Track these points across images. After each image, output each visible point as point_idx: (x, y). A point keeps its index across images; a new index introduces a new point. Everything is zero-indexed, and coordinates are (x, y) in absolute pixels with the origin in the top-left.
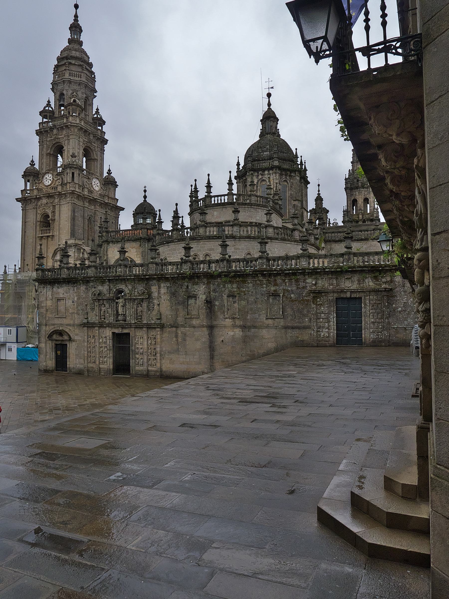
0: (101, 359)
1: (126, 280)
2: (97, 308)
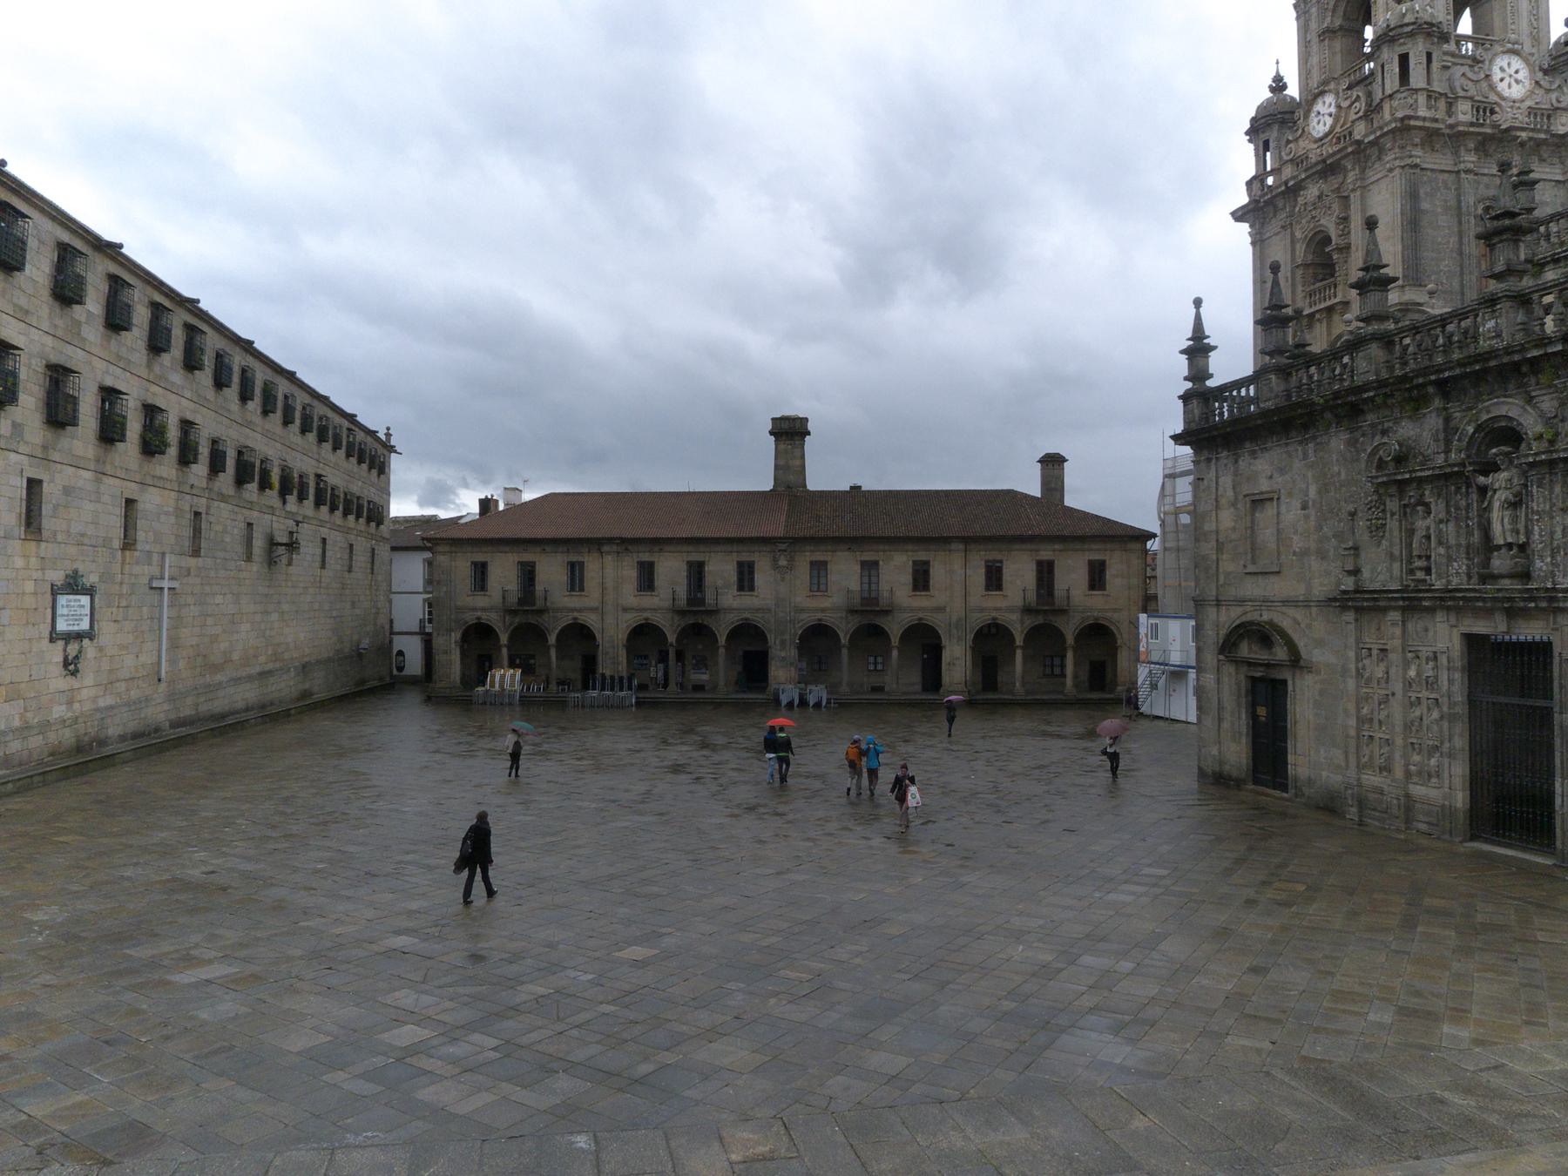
0: (1416, 758)
1: (1524, 369)
2: (1393, 524)
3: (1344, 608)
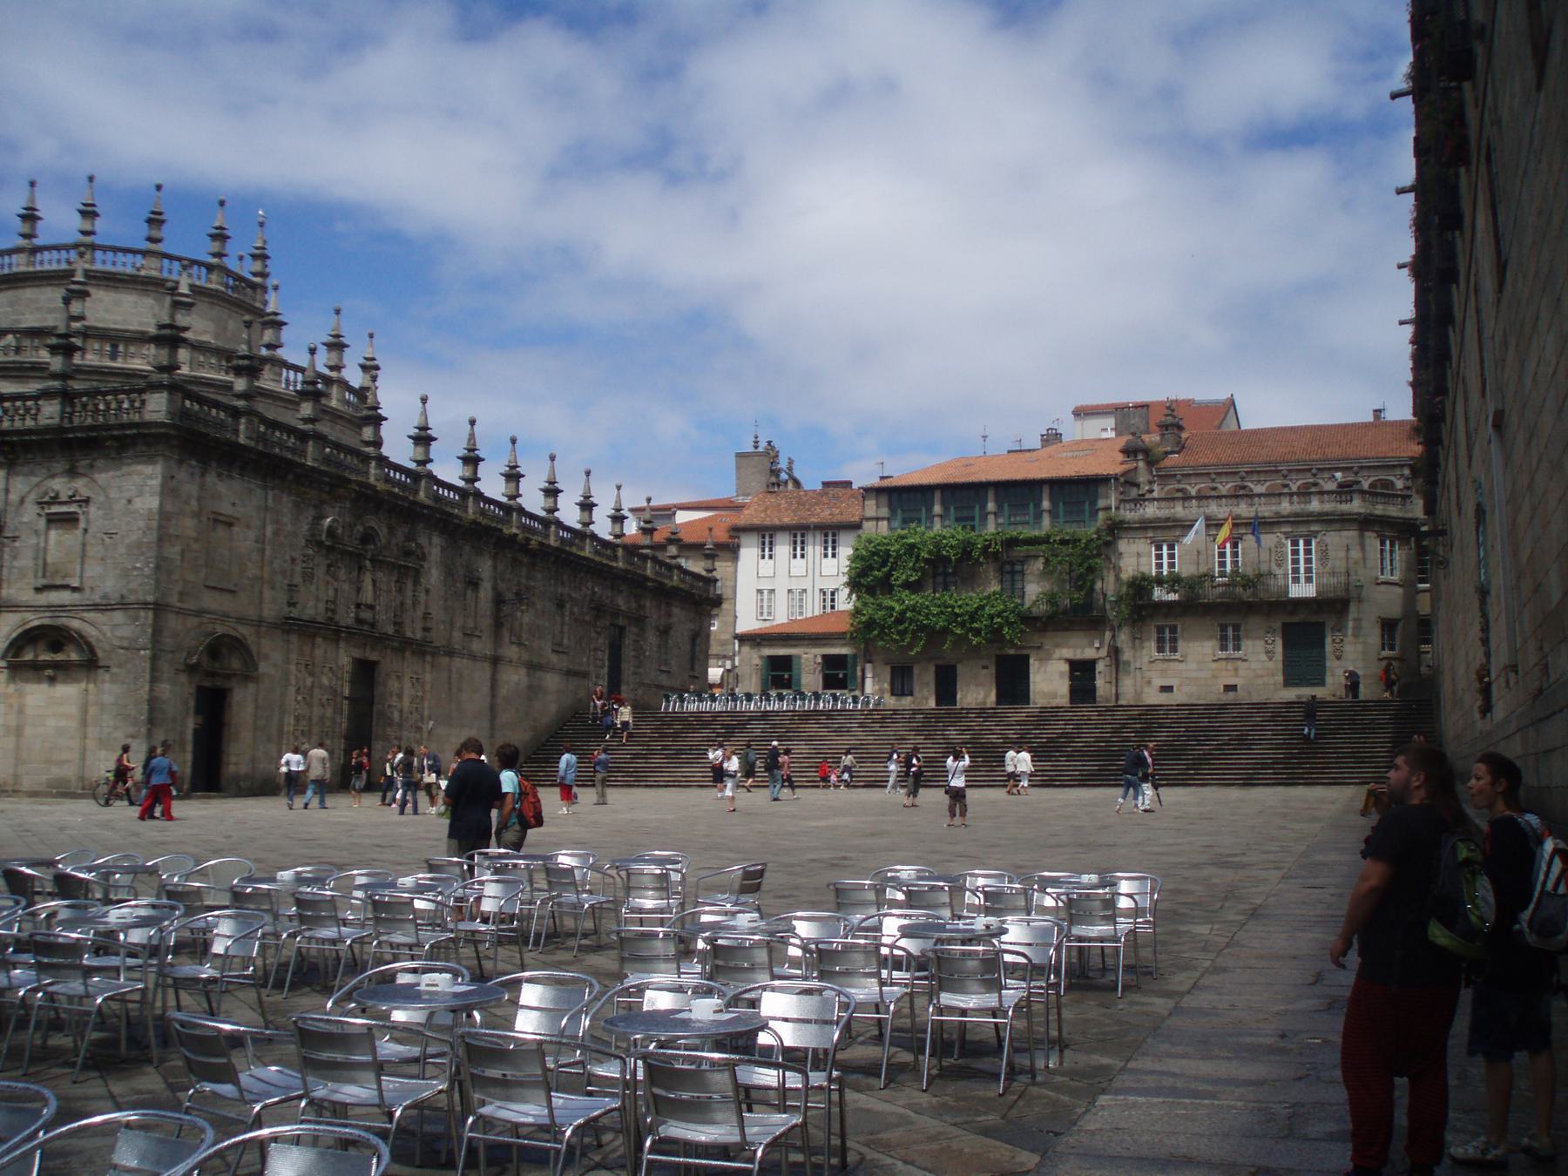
3: (288, 632)
